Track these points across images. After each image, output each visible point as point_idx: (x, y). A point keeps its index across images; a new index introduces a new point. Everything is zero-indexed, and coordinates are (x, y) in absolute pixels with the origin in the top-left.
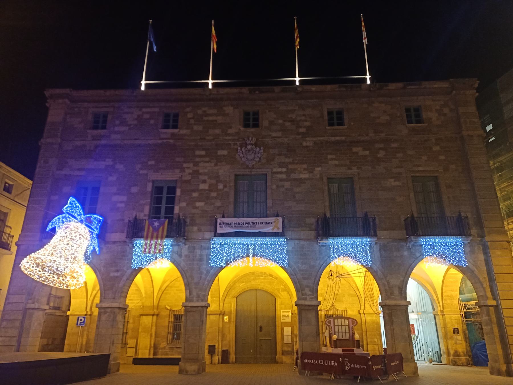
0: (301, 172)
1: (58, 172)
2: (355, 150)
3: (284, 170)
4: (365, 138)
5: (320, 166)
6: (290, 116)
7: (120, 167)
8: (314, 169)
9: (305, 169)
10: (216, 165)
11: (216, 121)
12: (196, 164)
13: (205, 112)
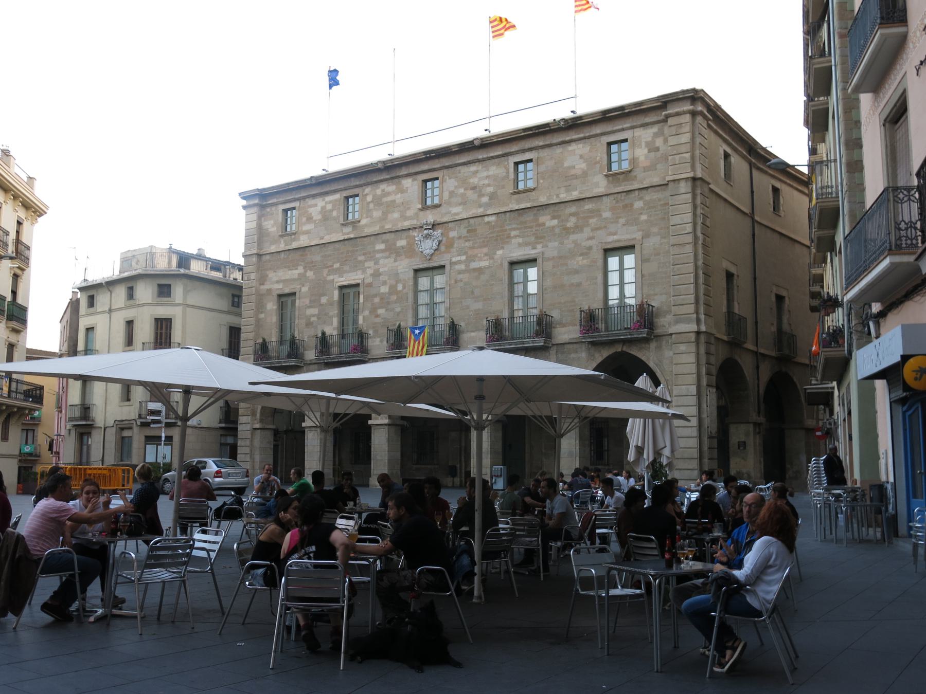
0: (481, 259)
1: (262, 287)
2: (542, 219)
3: (464, 258)
5: (503, 248)
6: (471, 181)
7: (310, 274)
8: (495, 254)
9: (486, 255)
10: (395, 261)
12: (376, 263)
13: (383, 191)
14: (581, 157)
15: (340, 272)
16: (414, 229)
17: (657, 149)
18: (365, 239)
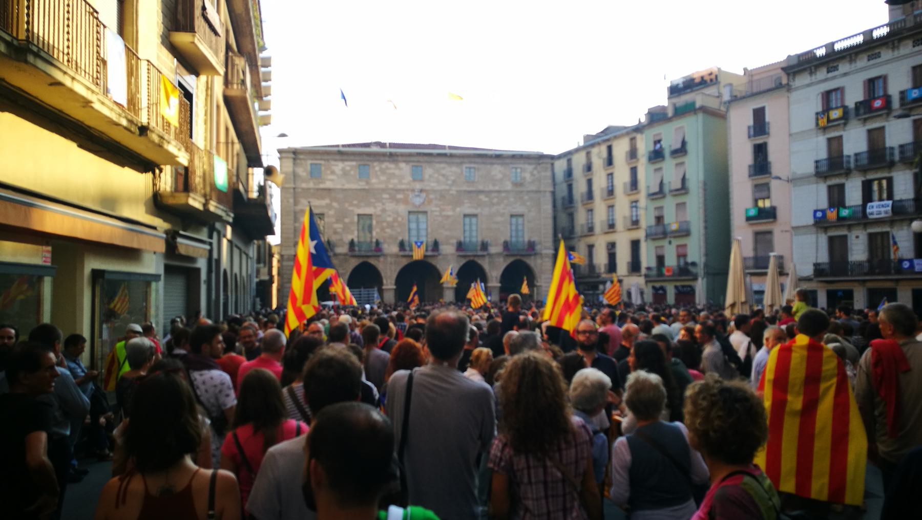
3: (438, 209)
4: (487, 189)
7: (335, 205)
15: (358, 206)
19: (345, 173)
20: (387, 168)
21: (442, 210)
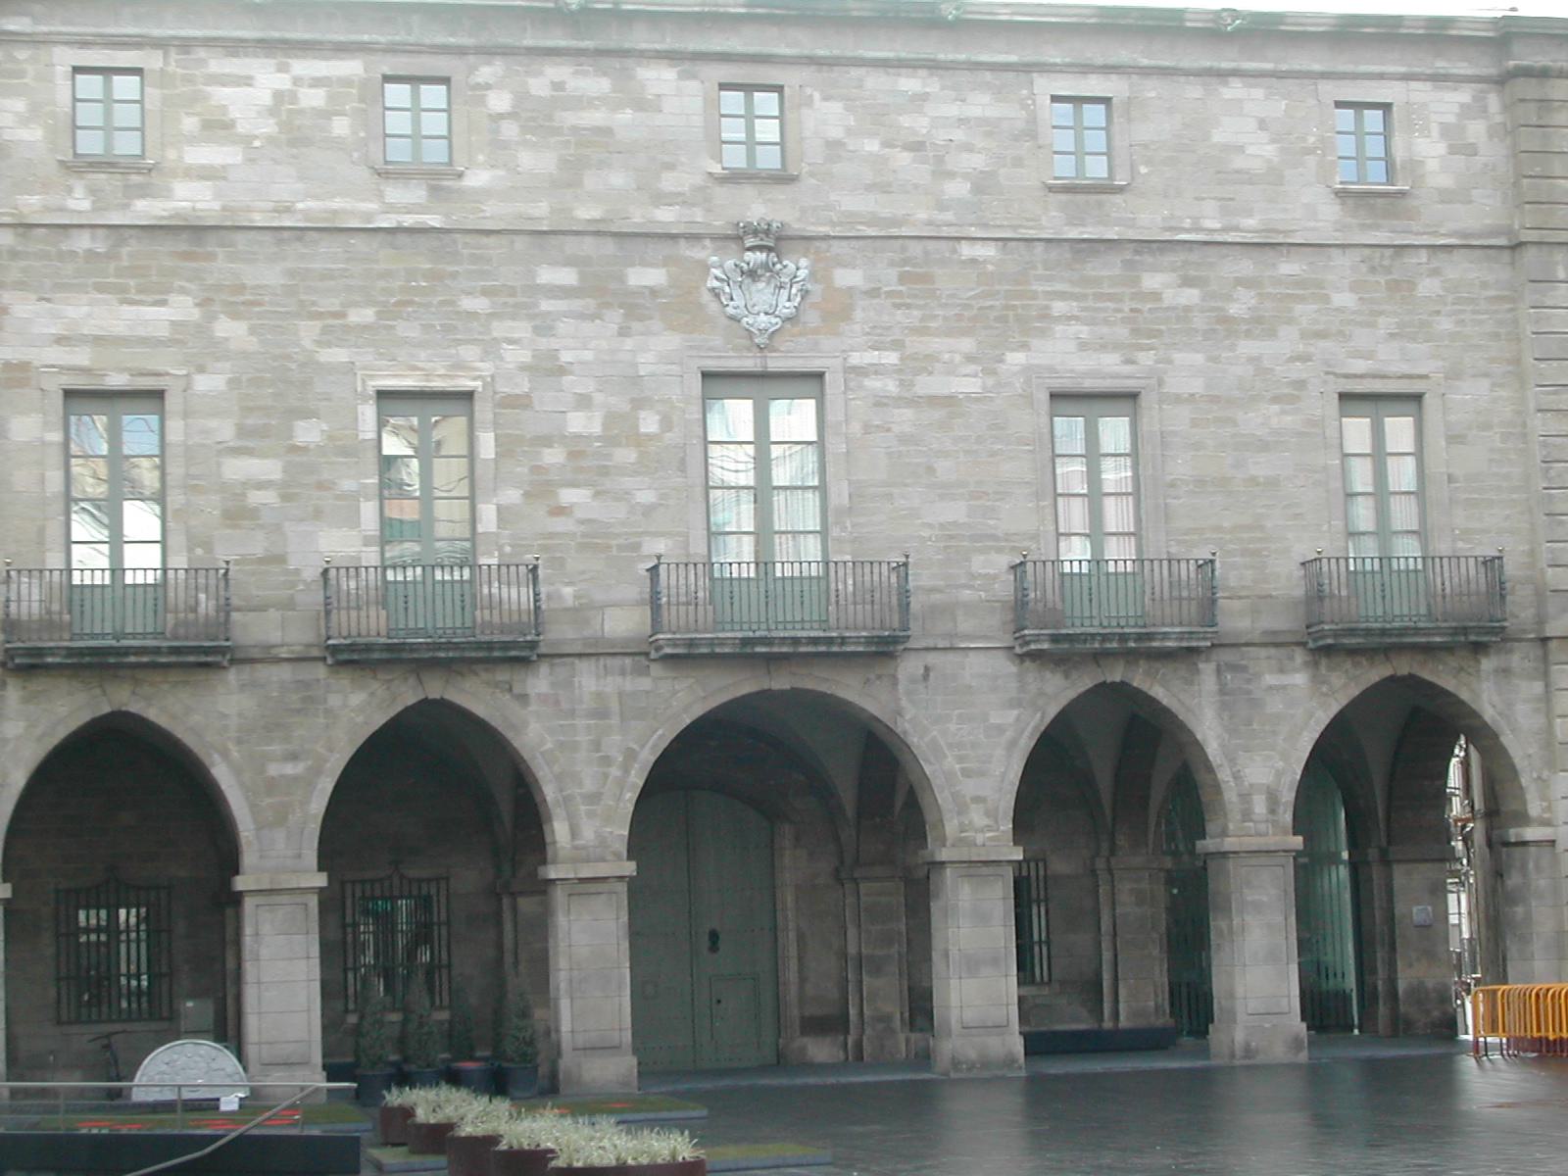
0: (951, 371)
2: (1151, 281)
3: (891, 358)
5: (1024, 347)
6: (905, 121)
7: (230, 330)
9: (970, 359)
10: (624, 332)
11: (607, 131)
12: (544, 326)
13: (558, 86)
14: (1262, 124)
16: (694, 238)
17: (1471, 150)
18: (491, 240)
19: (296, 134)
20: (561, 98)
21: (916, 365)
